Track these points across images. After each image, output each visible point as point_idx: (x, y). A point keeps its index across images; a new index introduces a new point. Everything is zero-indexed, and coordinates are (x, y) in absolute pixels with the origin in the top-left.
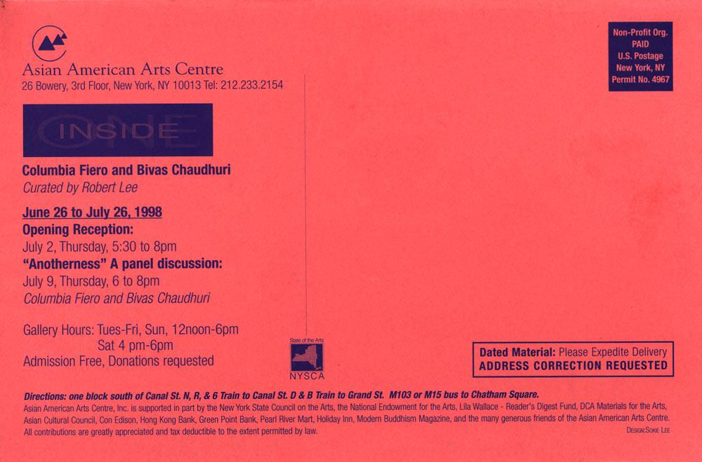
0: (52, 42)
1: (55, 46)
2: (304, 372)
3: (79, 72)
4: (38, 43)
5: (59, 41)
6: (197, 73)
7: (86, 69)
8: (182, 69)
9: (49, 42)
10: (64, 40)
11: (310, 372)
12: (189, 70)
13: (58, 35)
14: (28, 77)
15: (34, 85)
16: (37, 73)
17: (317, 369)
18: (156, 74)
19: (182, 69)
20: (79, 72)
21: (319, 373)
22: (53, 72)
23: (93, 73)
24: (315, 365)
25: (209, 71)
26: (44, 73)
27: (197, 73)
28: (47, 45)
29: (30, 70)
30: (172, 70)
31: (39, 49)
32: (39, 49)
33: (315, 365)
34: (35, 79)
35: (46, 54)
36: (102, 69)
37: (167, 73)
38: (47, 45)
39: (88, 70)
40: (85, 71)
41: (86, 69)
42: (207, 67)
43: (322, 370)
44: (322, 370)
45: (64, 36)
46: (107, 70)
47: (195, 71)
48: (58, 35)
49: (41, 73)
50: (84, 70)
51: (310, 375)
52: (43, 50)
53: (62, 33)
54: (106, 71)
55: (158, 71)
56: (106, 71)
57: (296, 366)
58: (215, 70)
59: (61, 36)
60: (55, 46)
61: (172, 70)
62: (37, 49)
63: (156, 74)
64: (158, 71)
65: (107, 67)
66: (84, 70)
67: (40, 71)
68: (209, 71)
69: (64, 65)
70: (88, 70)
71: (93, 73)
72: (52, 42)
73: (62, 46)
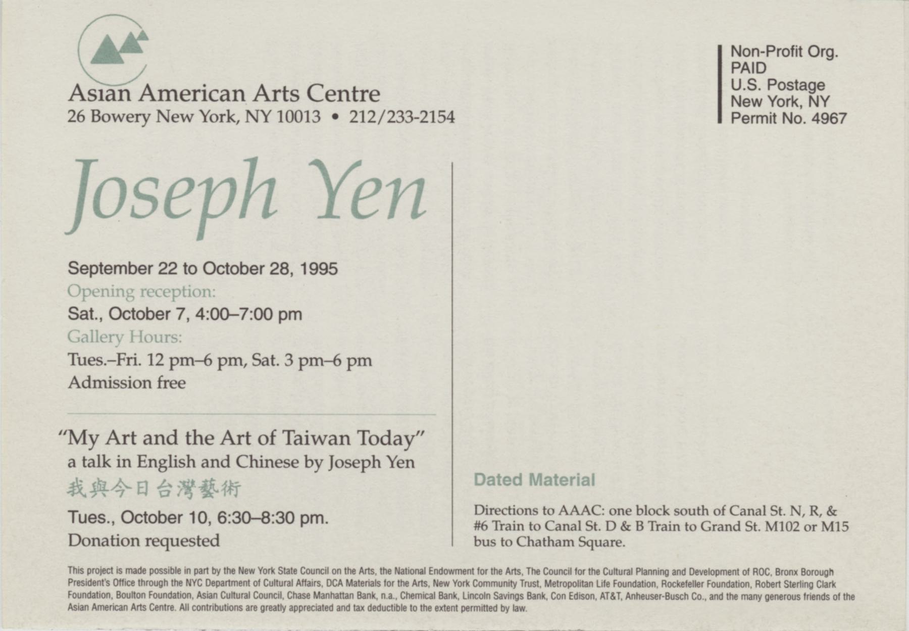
3: (156, 95)
4: (92, 45)
6: (340, 100)
7: (168, 92)
8: (317, 93)
10: (141, 43)
12: (327, 95)
14: (77, 105)
15: (88, 115)
16: (92, 98)
18: (275, 100)
20: (156, 95)
23: (179, 98)
25: (359, 96)
26: (104, 98)
27: (340, 100)
29: (81, 94)
30: (303, 94)
34: (87, 108)
36: (195, 92)
37: (294, 98)
39: (172, 94)
40: (167, 94)
41: (168, 92)
42: (354, 91)
45: (143, 36)
46: (202, 93)
49: (99, 98)
50: (165, 94)
52: (100, 62)
53: (140, 30)
54: (200, 96)
55: (280, 96)
56: (200, 96)
58: (367, 95)
59: (136, 36)
61: (303, 94)
62: (87, 58)
63: (275, 100)
64: (280, 96)
65: (203, 88)
66: (165, 94)
67: (98, 94)
68: (359, 96)
70: (172, 94)
71: (179, 98)
72: (118, 43)
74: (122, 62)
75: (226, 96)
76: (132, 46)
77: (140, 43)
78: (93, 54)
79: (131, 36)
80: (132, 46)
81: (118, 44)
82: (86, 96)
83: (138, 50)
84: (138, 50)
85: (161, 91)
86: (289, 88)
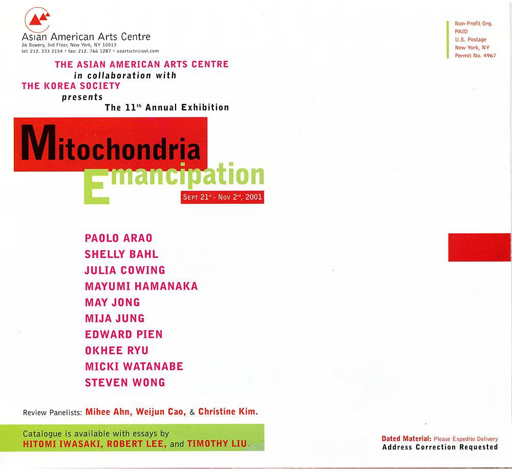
1: (41, 21)
4: (30, 19)
13: (43, 14)
19: (125, 36)
22: (39, 38)
25: (141, 37)
28: (35, 21)
31: (31, 24)
32: (31, 24)
35: (35, 28)
38: (35, 21)
39: (64, 37)
45: (48, 15)
47: (132, 38)
50: (60, 37)
54: (75, 38)
55: (109, 37)
56: (75, 38)
59: (45, 15)
61: (119, 37)
64: (109, 38)
65: (76, 35)
66: (60, 37)
68: (141, 37)
70: (64, 37)
72: (39, 17)
74: (40, 24)
75: (87, 38)
76: (43, 18)
77: (47, 17)
79: (43, 14)
80: (43, 18)
81: (39, 18)
83: (46, 19)
84: (46, 19)
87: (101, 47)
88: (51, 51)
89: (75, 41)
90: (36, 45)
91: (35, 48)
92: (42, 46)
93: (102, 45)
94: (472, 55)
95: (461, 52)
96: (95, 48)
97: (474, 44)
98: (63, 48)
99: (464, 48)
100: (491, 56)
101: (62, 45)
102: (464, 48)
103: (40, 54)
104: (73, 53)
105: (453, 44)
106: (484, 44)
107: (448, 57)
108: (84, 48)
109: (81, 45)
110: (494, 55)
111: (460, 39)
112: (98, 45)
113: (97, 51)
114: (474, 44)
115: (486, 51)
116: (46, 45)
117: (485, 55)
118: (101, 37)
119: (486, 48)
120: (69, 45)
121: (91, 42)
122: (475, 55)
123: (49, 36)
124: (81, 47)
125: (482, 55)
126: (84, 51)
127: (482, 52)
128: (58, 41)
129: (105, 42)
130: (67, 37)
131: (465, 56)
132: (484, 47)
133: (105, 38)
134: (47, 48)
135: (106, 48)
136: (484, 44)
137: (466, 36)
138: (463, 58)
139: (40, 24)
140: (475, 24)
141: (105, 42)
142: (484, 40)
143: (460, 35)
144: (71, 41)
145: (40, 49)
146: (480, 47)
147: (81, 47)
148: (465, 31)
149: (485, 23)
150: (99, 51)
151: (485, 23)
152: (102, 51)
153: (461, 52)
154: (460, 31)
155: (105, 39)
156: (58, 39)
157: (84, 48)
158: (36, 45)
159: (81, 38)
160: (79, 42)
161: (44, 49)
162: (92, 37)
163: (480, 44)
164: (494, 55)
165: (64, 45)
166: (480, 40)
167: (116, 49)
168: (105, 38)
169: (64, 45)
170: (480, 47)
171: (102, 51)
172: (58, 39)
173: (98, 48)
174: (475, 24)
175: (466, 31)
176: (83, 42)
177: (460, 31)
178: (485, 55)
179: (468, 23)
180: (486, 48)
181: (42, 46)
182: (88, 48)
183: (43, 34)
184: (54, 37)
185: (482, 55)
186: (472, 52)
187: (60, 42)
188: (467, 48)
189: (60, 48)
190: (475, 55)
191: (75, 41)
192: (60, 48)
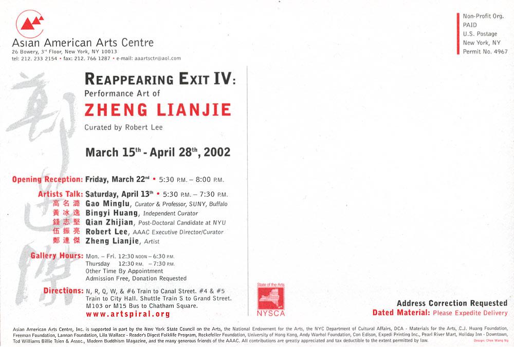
0: (32, 22)
1: (34, 26)
2: (268, 311)
4: (21, 23)
5: (37, 21)
9: (29, 21)
11: (273, 311)
13: (36, 18)
16: (22, 45)
17: (279, 307)
21: (280, 311)
22: (32, 44)
24: (277, 305)
28: (28, 25)
29: (18, 44)
31: (23, 28)
32: (23, 28)
33: (277, 305)
35: (28, 32)
38: (28, 25)
39: (58, 43)
43: (282, 308)
44: (282, 308)
48: (36, 18)
50: (55, 43)
51: (273, 313)
54: (71, 44)
57: (263, 305)
60: (34, 26)
62: (20, 28)
65: (72, 40)
66: (55, 43)
69: (42, 42)
70: (58, 43)
72: (32, 22)
73: (39, 25)
75: (84, 44)
78: (22, 26)
82: (20, 44)
85: (53, 42)
86: (112, 40)
87: (100, 54)
88: (44, 59)
89: (70, 48)
90: (28, 52)
91: (27, 55)
92: (35, 53)
93: (100, 52)
94: (482, 51)
95: (469, 48)
96: (92, 55)
97: (483, 39)
98: (58, 56)
99: (472, 43)
100: (502, 52)
101: (55, 52)
102: (472, 43)
103: (32, 62)
104: (69, 61)
105: (462, 38)
106: (495, 38)
107: (458, 53)
108: (80, 55)
109: (76, 52)
110: (505, 51)
111: (468, 34)
112: (96, 52)
113: (95, 59)
114: (483, 39)
115: (497, 47)
116: (40, 52)
117: (496, 52)
118: (99, 42)
119: (497, 43)
120: (63, 52)
121: (89, 49)
122: (485, 52)
123: (42, 43)
124: (77, 54)
125: (492, 51)
126: (80, 58)
127: (492, 48)
128: (52, 48)
129: (104, 48)
130: (62, 43)
131: (474, 51)
132: (494, 42)
133: (104, 44)
134: (40, 55)
135: (104, 55)
136: (495, 38)
137: (474, 31)
138: (471, 55)
139: (33, 29)
140: (486, 16)
141: (104, 48)
142: (495, 34)
143: (468, 29)
144: (66, 48)
145: (32, 56)
146: (490, 42)
147: (77, 54)
148: (474, 25)
149: (495, 16)
150: (98, 59)
151: (495, 16)
152: (101, 58)
153: (469, 48)
154: (468, 25)
155: (104, 45)
156: (52, 45)
157: (80, 55)
158: (28, 52)
159: (78, 44)
160: (75, 48)
161: (37, 56)
162: (89, 43)
163: (490, 39)
164: (505, 51)
165: (58, 52)
166: (490, 34)
167: (115, 56)
168: (104, 44)
169: (58, 52)
170: (490, 42)
171: (101, 58)
172: (52, 45)
173: (96, 55)
174: (486, 16)
175: (475, 26)
176: (80, 48)
177: (468, 25)
178: (496, 52)
179: (478, 15)
180: (497, 43)
181: (35, 53)
182: (85, 55)
183: (36, 39)
184: (48, 43)
185: (492, 51)
186: (482, 47)
187: (55, 48)
188: (476, 43)
189: (55, 55)
190: (485, 52)
191: (70, 48)
192: (55, 55)
